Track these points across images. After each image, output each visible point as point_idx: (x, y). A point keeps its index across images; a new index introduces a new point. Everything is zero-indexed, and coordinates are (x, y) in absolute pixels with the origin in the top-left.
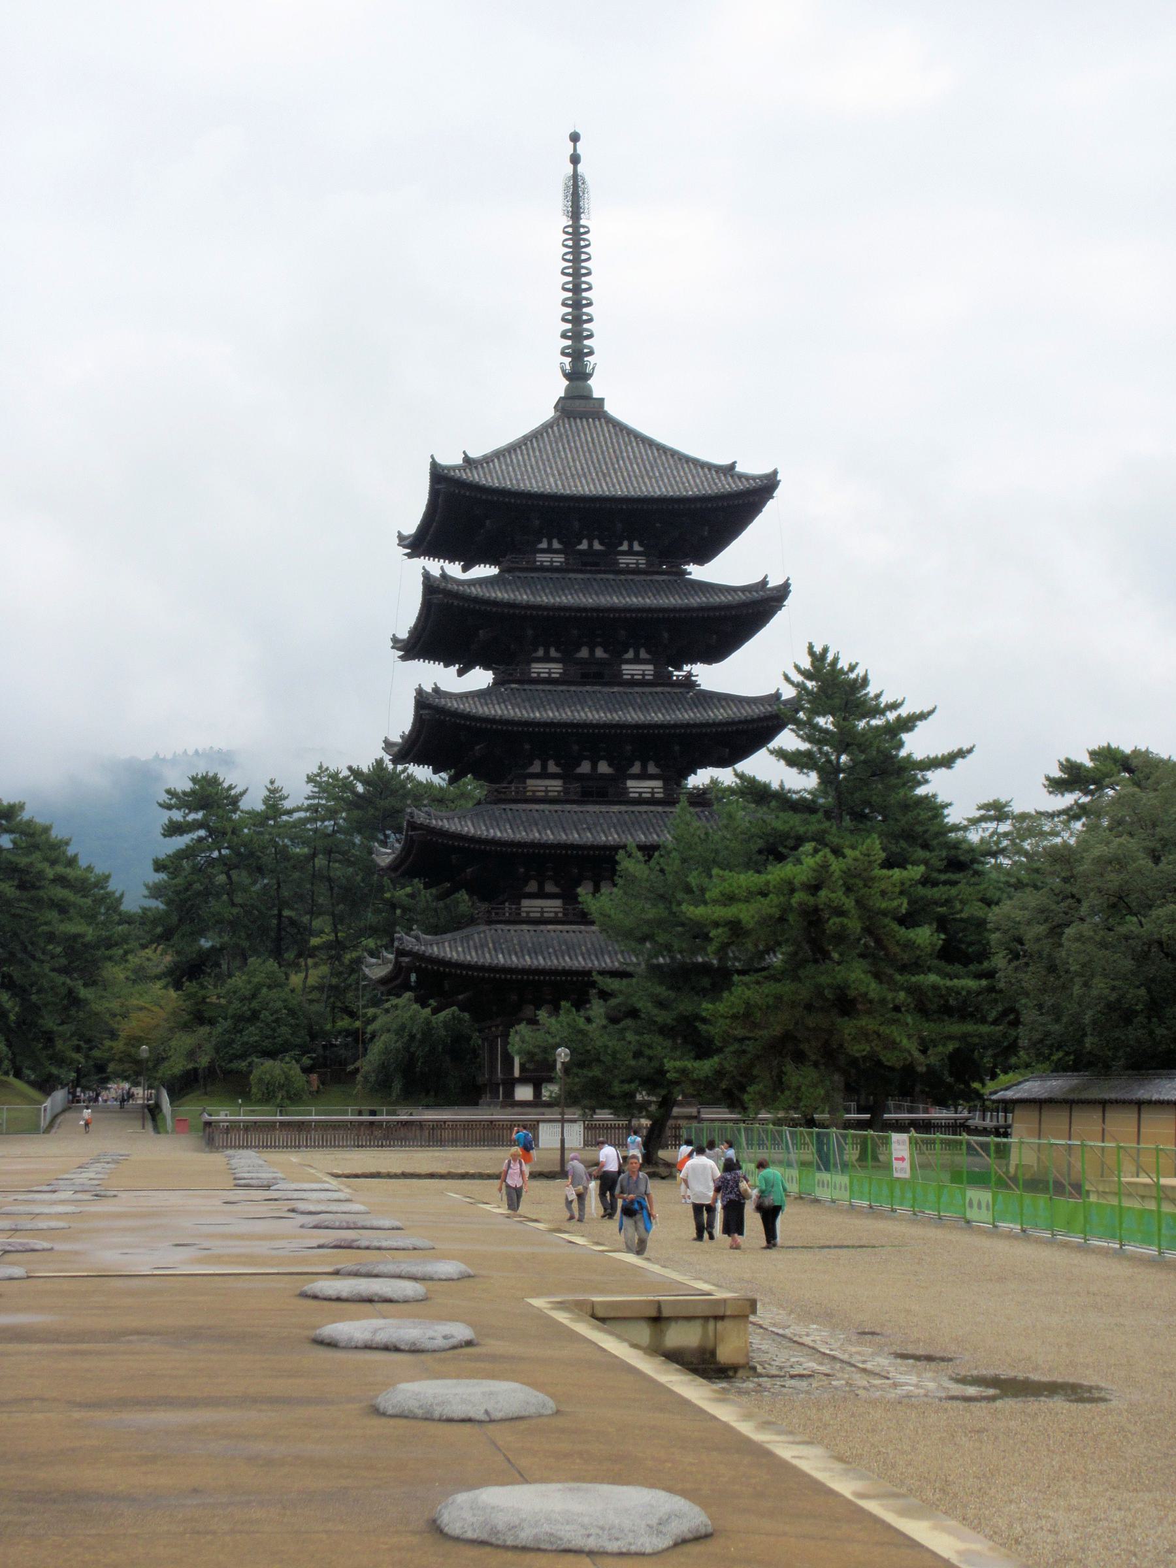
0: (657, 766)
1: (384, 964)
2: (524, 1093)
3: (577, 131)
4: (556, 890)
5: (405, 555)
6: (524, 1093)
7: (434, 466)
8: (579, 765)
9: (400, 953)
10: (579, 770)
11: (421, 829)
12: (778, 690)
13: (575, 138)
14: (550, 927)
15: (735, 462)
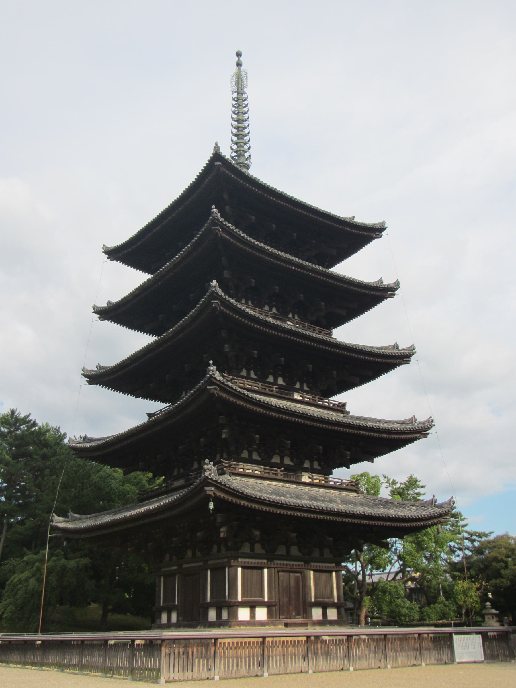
0: (308, 387)
1: (72, 521)
2: (244, 614)
3: (242, 52)
4: (259, 458)
5: (107, 257)
6: (244, 614)
7: (217, 148)
8: (268, 377)
9: (207, 482)
10: (268, 380)
11: (218, 386)
12: (396, 343)
13: (239, 55)
14: (268, 482)
15: (354, 217)
